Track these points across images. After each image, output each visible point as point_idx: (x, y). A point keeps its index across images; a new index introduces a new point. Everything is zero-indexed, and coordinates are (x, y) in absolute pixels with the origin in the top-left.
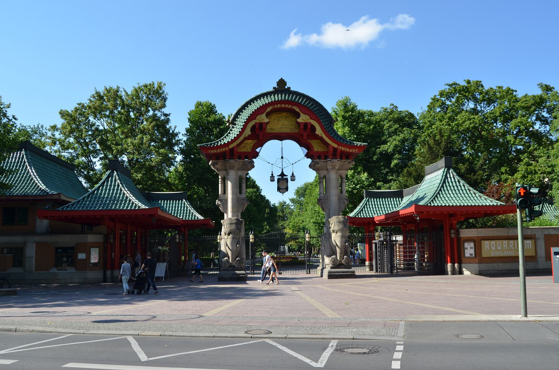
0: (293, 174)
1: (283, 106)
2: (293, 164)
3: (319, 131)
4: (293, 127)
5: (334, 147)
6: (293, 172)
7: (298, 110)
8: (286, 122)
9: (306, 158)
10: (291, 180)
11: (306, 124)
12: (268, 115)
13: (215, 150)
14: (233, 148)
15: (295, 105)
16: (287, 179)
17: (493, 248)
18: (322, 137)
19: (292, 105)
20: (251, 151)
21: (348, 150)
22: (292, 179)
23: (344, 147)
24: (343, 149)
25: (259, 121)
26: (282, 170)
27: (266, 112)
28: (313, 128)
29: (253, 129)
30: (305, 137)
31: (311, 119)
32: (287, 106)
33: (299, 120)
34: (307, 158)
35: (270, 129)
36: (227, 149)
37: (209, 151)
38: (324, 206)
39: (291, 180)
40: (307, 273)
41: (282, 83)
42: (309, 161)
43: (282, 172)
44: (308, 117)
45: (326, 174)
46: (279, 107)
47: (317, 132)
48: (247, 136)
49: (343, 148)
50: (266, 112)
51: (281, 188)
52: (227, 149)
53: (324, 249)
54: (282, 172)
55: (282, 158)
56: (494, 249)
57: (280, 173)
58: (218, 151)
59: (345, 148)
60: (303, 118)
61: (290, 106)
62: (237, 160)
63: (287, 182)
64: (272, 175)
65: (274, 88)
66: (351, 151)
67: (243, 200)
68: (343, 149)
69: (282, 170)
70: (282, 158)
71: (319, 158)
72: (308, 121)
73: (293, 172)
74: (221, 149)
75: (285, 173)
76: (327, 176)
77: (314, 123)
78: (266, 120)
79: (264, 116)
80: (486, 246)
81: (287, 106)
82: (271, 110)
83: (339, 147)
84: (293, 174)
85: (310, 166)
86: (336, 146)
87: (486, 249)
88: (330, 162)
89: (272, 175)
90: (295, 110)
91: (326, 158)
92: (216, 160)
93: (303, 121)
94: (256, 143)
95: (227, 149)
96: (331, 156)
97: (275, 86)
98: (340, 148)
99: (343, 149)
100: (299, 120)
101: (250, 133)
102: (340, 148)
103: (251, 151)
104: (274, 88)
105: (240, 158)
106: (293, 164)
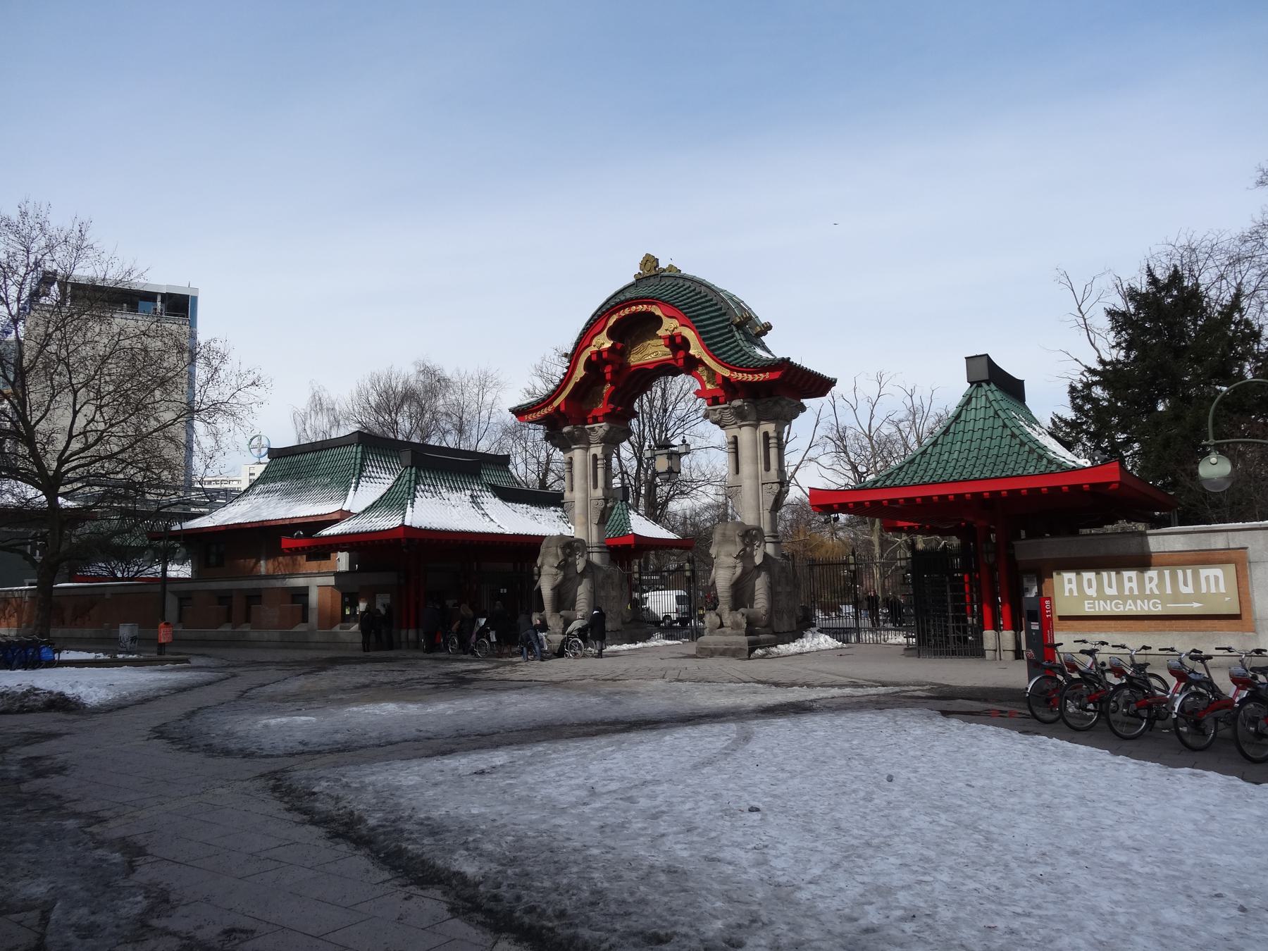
5: (723, 377)
7: (658, 312)
14: (559, 406)
17: (1092, 592)
25: (596, 349)
28: (685, 343)
29: (588, 363)
36: (550, 409)
49: (740, 374)
52: (550, 409)
56: (1095, 595)
59: (745, 375)
80: (1067, 587)
86: (726, 373)
87: (1067, 594)
98: (735, 375)
101: (584, 373)
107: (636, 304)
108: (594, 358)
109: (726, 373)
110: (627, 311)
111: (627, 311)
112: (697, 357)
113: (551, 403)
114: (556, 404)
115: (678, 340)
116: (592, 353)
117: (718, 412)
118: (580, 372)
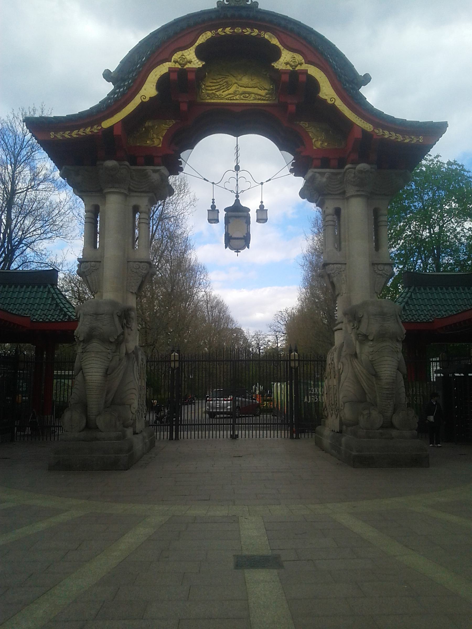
0: (262, 207)
1: (238, 30)
2: (262, 183)
4: (263, 93)
5: (364, 132)
6: (262, 202)
7: (275, 41)
8: (245, 80)
9: (292, 175)
10: (258, 220)
13: (67, 132)
14: (111, 128)
15: (267, 29)
16: (247, 219)
18: (333, 107)
20: (160, 146)
22: (260, 218)
25: (177, 66)
26: (237, 196)
27: (196, 44)
30: (292, 108)
31: (308, 62)
32: (247, 31)
33: (280, 65)
34: (295, 175)
35: (208, 94)
36: (96, 129)
38: (335, 280)
39: (258, 220)
42: (300, 182)
43: (237, 201)
44: (299, 58)
45: (341, 207)
46: (228, 32)
47: (321, 95)
48: (147, 99)
49: (386, 132)
50: (196, 44)
54: (237, 201)
55: (237, 168)
57: (231, 203)
62: (127, 163)
63: (248, 222)
64: (213, 207)
66: (407, 141)
67: (141, 262)
69: (237, 196)
70: (237, 168)
71: (325, 163)
73: (262, 202)
74: (82, 130)
75: (244, 203)
76: (342, 211)
77: (313, 71)
78: (197, 64)
81: (247, 31)
82: (209, 41)
83: (377, 131)
84: (262, 207)
85: (303, 194)
86: (368, 127)
88: (353, 170)
89: (213, 207)
90: (268, 42)
91: (341, 164)
93: (289, 67)
95: (96, 131)
99: (386, 137)
102: (380, 132)
103: (160, 146)
105: (134, 162)
106: (262, 183)
108: (174, 76)
110: (228, 30)
111: (228, 30)
112: (329, 102)
113: (99, 122)
114: (106, 124)
115: (302, 78)
116: (171, 70)
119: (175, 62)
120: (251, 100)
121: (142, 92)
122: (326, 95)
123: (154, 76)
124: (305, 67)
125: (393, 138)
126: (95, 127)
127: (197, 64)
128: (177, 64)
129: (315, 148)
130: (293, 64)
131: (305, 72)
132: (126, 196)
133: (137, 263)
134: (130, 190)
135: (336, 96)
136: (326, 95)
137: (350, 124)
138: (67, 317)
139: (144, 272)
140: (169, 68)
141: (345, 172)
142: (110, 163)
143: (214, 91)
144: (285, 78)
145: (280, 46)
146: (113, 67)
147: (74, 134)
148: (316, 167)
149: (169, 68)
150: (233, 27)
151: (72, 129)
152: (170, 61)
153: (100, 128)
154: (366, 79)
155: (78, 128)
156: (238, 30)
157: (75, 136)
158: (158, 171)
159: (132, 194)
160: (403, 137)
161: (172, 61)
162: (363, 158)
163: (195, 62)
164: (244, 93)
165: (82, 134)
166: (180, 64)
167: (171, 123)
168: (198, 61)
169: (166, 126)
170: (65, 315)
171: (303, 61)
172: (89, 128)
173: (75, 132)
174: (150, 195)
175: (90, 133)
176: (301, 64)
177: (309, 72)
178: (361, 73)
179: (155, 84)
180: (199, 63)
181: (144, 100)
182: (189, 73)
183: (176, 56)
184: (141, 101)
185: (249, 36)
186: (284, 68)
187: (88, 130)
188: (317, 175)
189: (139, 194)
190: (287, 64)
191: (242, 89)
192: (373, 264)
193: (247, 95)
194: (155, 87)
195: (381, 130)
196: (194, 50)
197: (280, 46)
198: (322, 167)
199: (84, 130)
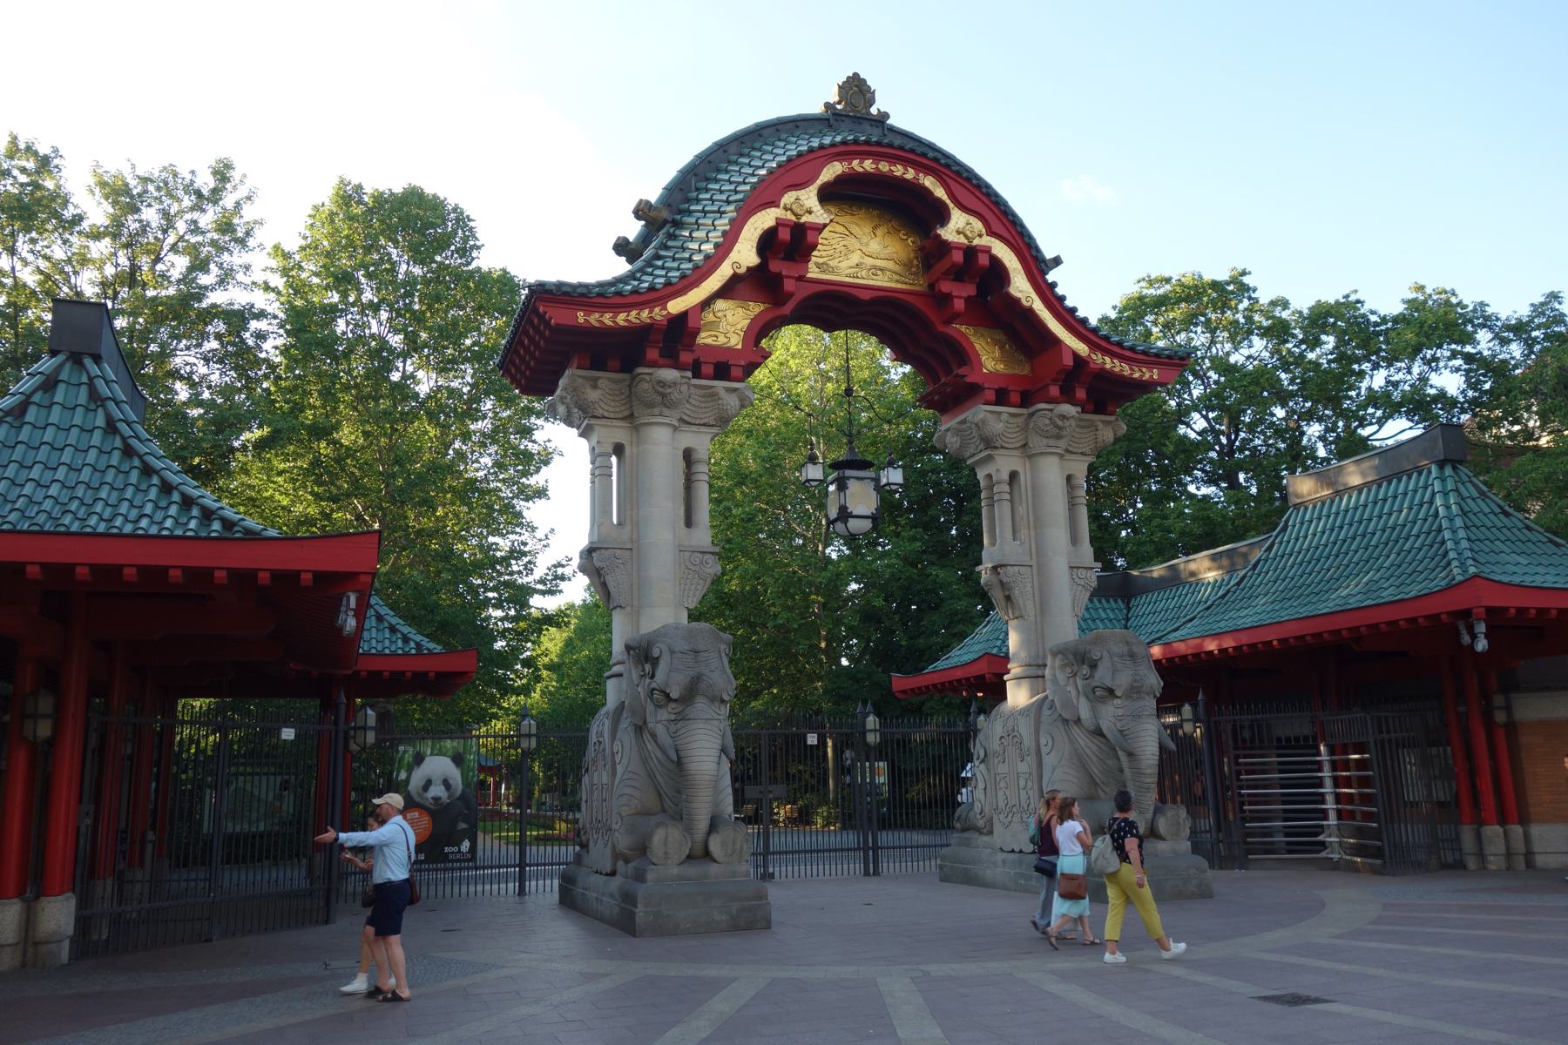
1: (884, 167)
3: (1020, 286)
5: (1075, 355)
7: (940, 193)
8: (875, 245)
11: (971, 252)
12: (827, 195)
13: (608, 315)
14: (683, 316)
15: (929, 171)
18: (1030, 311)
19: (919, 167)
20: (739, 347)
21: (1126, 370)
23: (1113, 355)
24: (1108, 363)
27: (819, 182)
28: (998, 272)
29: (767, 243)
31: (991, 233)
32: (898, 170)
33: (948, 233)
37: (580, 314)
40: (867, 873)
41: (856, 89)
44: (978, 225)
45: (1020, 469)
46: (868, 169)
47: (1013, 290)
48: (742, 270)
49: (1108, 359)
50: (819, 182)
51: (855, 513)
53: (605, 779)
58: (621, 319)
60: (959, 227)
61: (910, 174)
65: (828, 106)
66: (1137, 375)
68: (1108, 363)
71: (1001, 398)
72: (976, 242)
74: (634, 313)
78: (819, 215)
79: (808, 197)
81: (898, 170)
82: (840, 180)
83: (1094, 357)
86: (1081, 348)
90: (927, 192)
92: (591, 368)
93: (962, 240)
94: (761, 313)
95: (658, 318)
96: (1054, 391)
97: (833, 97)
98: (1098, 358)
100: (948, 233)
102: (1098, 358)
103: (739, 347)
104: (828, 106)
107: (894, 159)
108: (785, 235)
109: (1081, 348)
110: (868, 165)
111: (868, 165)
112: (1024, 302)
114: (676, 306)
115: (983, 260)
116: (780, 223)
117: (1005, 417)
118: (745, 254)
119: (786, 209)
120: (882, 281)
121: (734, 256)
122: (1020, 291)
123: (752, 230)
124: (987, 241)
125: (1117, 369)
126: (657, 310)
127: (819, 215)
128: (789, 212)
129: (985, 371)
130: (970, 235)
131: (987, 250)
132: (675, 428)
133: (696, 554)
134: (681, 420)
135: (1034, 295)
136: (1020, 291)
137: (1057, 342)
138: (412, 645)
139: (707, 570)
140: (777, 218)
141: (1032, 414)
142: (669, 374)
143: (825, 259)
144: (958, 257)
145: (948, 202)
146: (653, 195)
147: (621, 319)
148: (987, 403)
149: (777, 218)
150: (876, 162)
151: (616, 308)
152: (778, 206)
153: (665, 313)
154: (1057, 261)
155: (627, 307)
156: (884, 167)
157: (622, 323)
158: (735, 390)
159: (685, 428)
160: (1131, 369)
161: (782, 205)
162: (1067, 396)
163: (818, 214)
164: (875, 267)
165: (633, 320)
166: (795, 215)
167: (761, 307)
168: (822, 211)
169: (749, 312)
170: (406, 640)
171: (984, 230)
172: (647, 311)
173: (622, 316)
174: (715, 430)
175: (648, 321)
176: (980, 236)
177: (994, 252)
178: (1049, 254)
179: (755, 245)
180: (825, 215)
181: (738, 271)
182: (809, 232)
183: (788, 198)
184: (732, 272)
185: (902, 180)
186: (956, 240)
187: (645, 314)
188: (989, 415)
189: (693, 428)
190: (959, 233)
191: (869, 261)
192: (1071, 567)
193: (879, 272)
194: (754, 250)
195: (1100, 356)
196: (816, 192)
197: (948, 202)
198: (996, 404)
199: (638, 314)
